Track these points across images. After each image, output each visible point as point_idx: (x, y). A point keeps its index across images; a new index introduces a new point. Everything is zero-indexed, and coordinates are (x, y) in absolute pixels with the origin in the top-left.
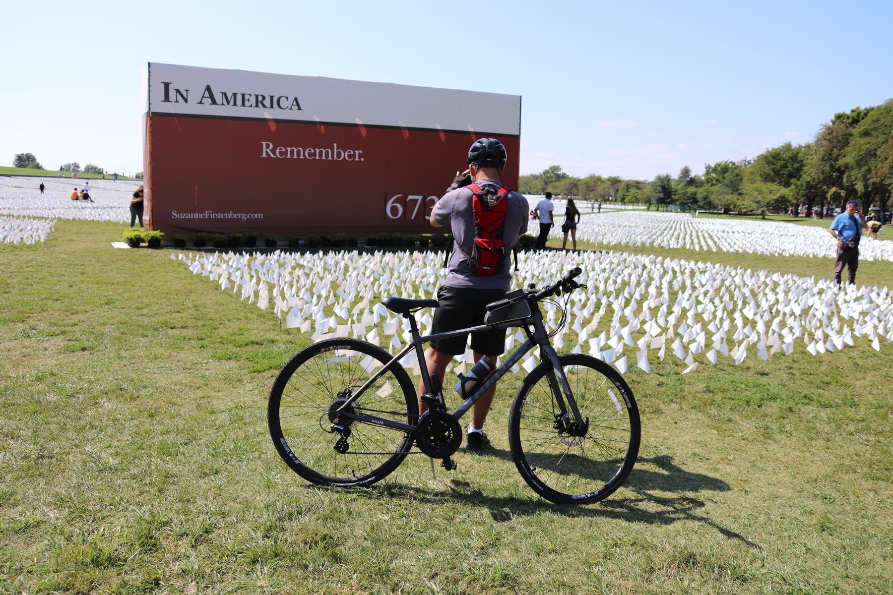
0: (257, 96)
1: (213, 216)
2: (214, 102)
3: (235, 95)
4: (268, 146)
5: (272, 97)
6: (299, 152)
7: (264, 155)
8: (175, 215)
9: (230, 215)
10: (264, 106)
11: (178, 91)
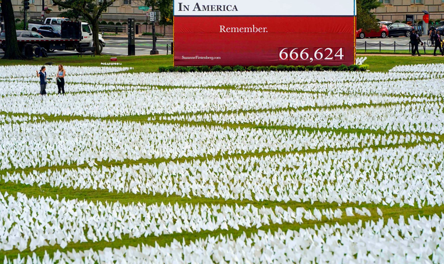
0: (218, 6)
1: (199, 58)
2: (199, 10)
3: (208, 6)
4: (222, 27)
5: (224, 6)
6: (236, 29)
7: (221, 31)
8: (183, 58)
9: (206, 58)
10: (221, 10)
11: (185, 6)
